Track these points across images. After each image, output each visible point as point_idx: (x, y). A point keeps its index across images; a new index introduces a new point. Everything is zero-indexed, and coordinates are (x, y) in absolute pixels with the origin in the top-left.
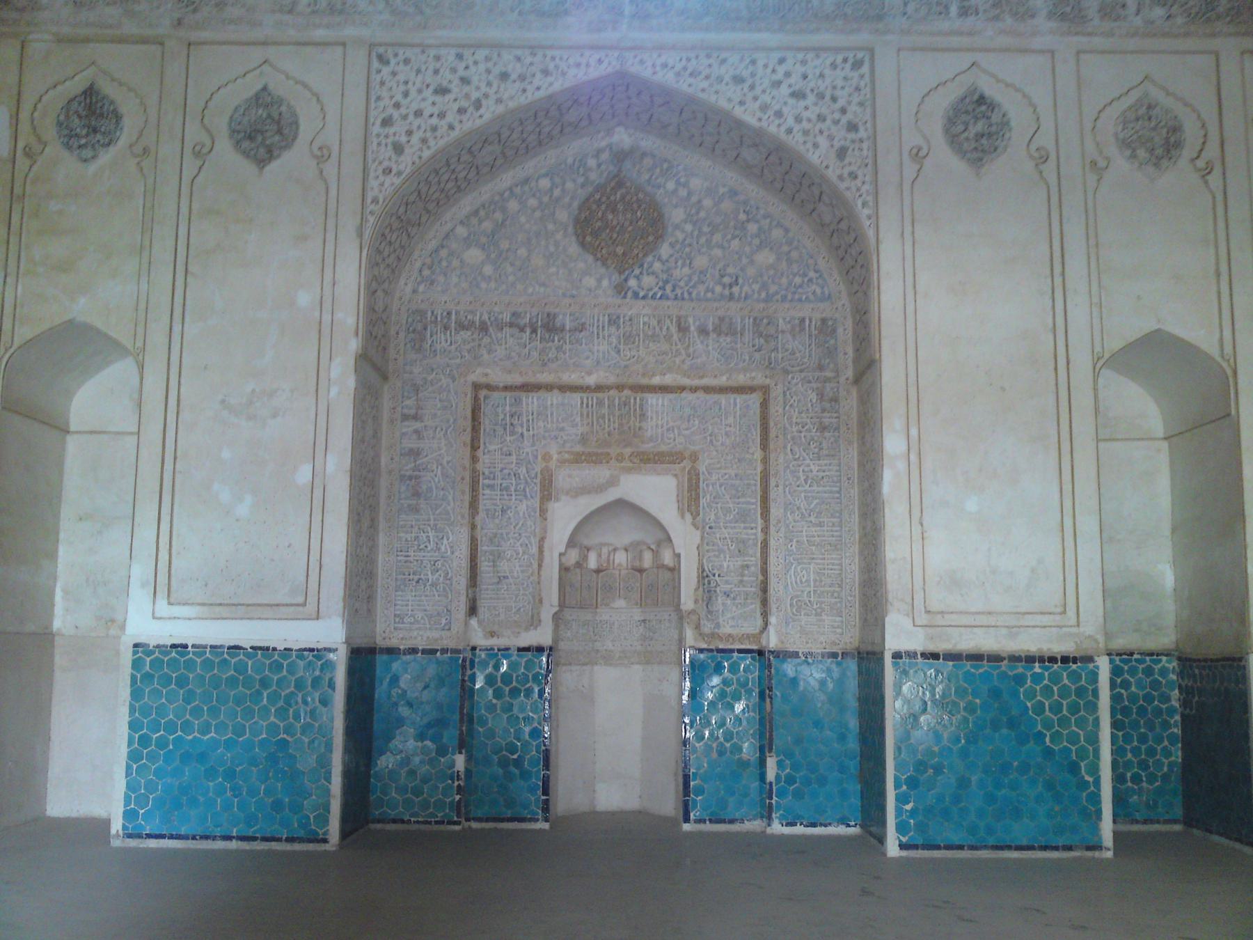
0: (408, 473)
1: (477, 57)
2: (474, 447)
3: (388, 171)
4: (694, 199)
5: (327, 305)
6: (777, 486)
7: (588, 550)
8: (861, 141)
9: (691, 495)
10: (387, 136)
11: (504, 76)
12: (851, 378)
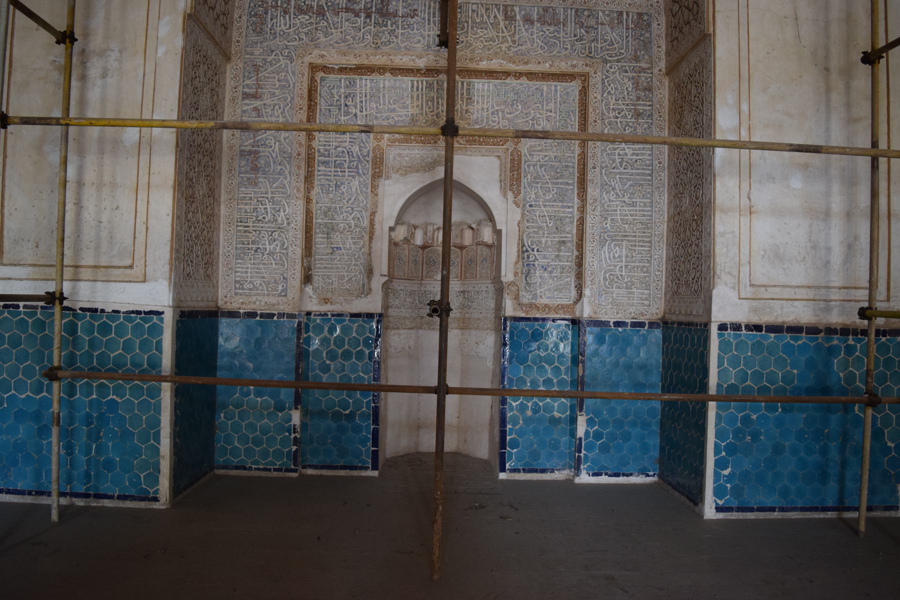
6: (594, 168)
7: (415, 229)
9: (513, 175)
12: (664, 70)
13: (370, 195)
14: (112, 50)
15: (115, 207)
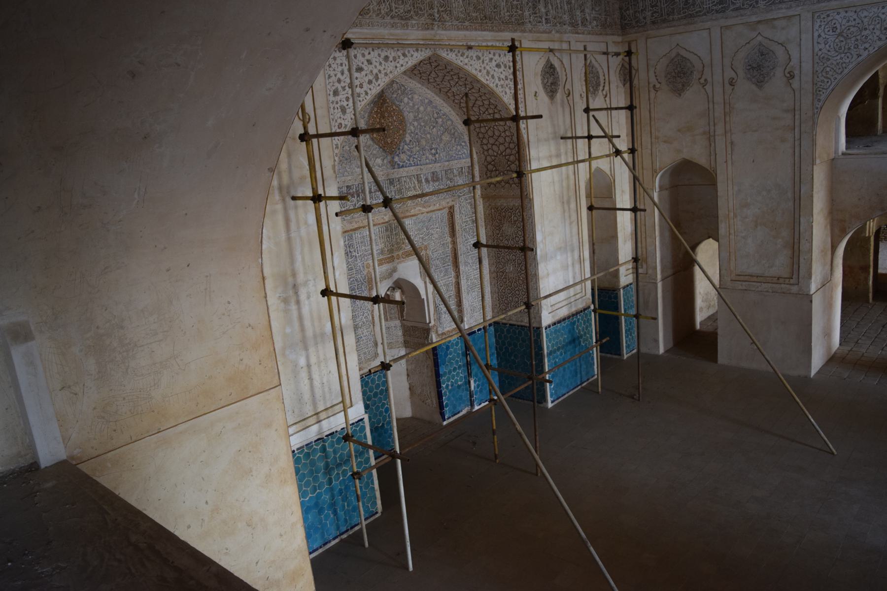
10: (337, 103)
14: (310, 280)
15: (329, 372)
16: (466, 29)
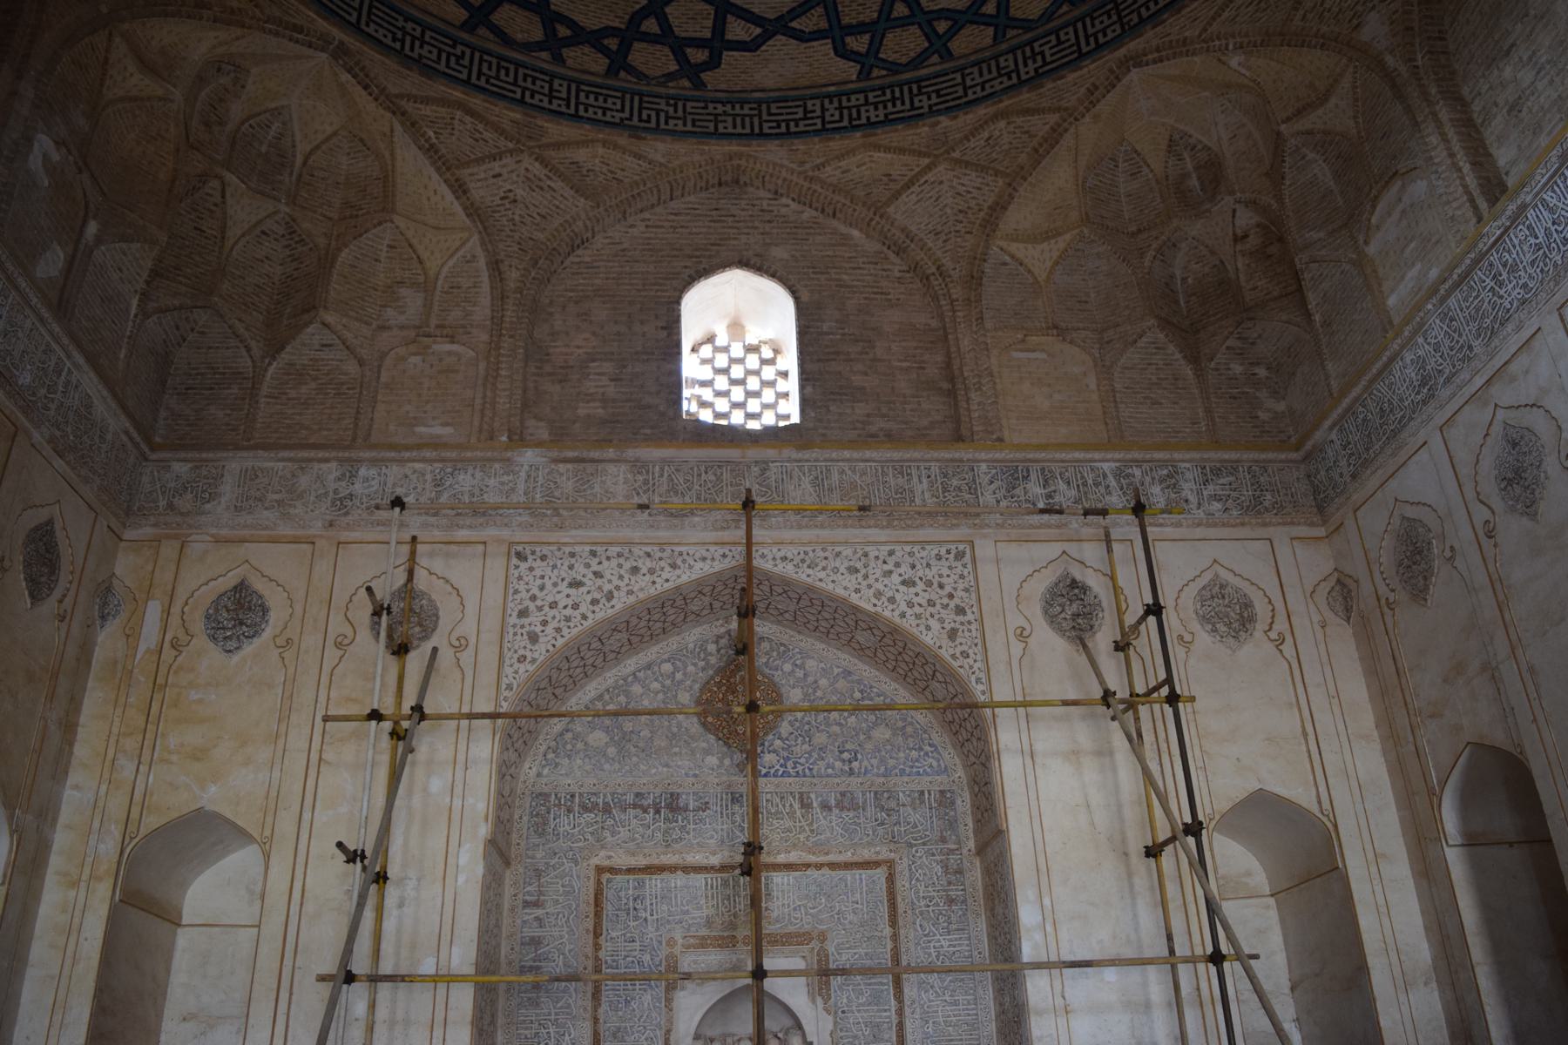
0: (528, 964)
1: (609, 554)
2: (597, 934)
3: (521, 659)
4: (810, 679)
5: (458, 790)
8: (969, 623)
10: (522, 627)
11: (635, 570)
13: (664, 1010)
16: (822, 527)
